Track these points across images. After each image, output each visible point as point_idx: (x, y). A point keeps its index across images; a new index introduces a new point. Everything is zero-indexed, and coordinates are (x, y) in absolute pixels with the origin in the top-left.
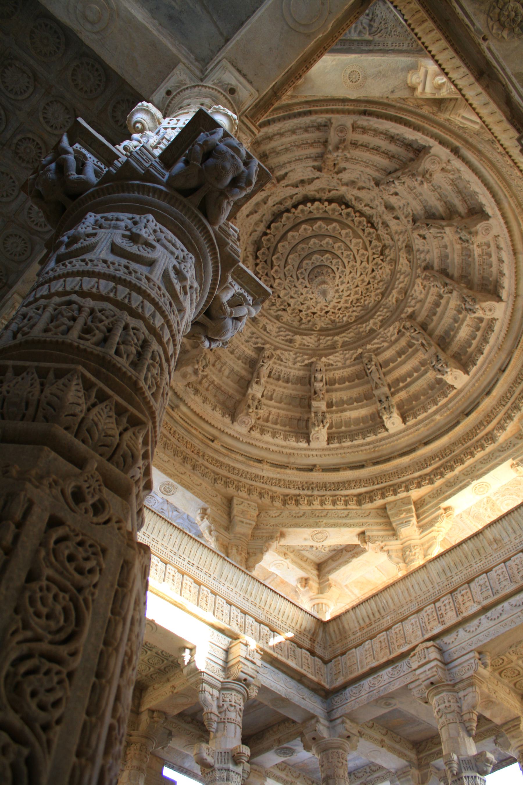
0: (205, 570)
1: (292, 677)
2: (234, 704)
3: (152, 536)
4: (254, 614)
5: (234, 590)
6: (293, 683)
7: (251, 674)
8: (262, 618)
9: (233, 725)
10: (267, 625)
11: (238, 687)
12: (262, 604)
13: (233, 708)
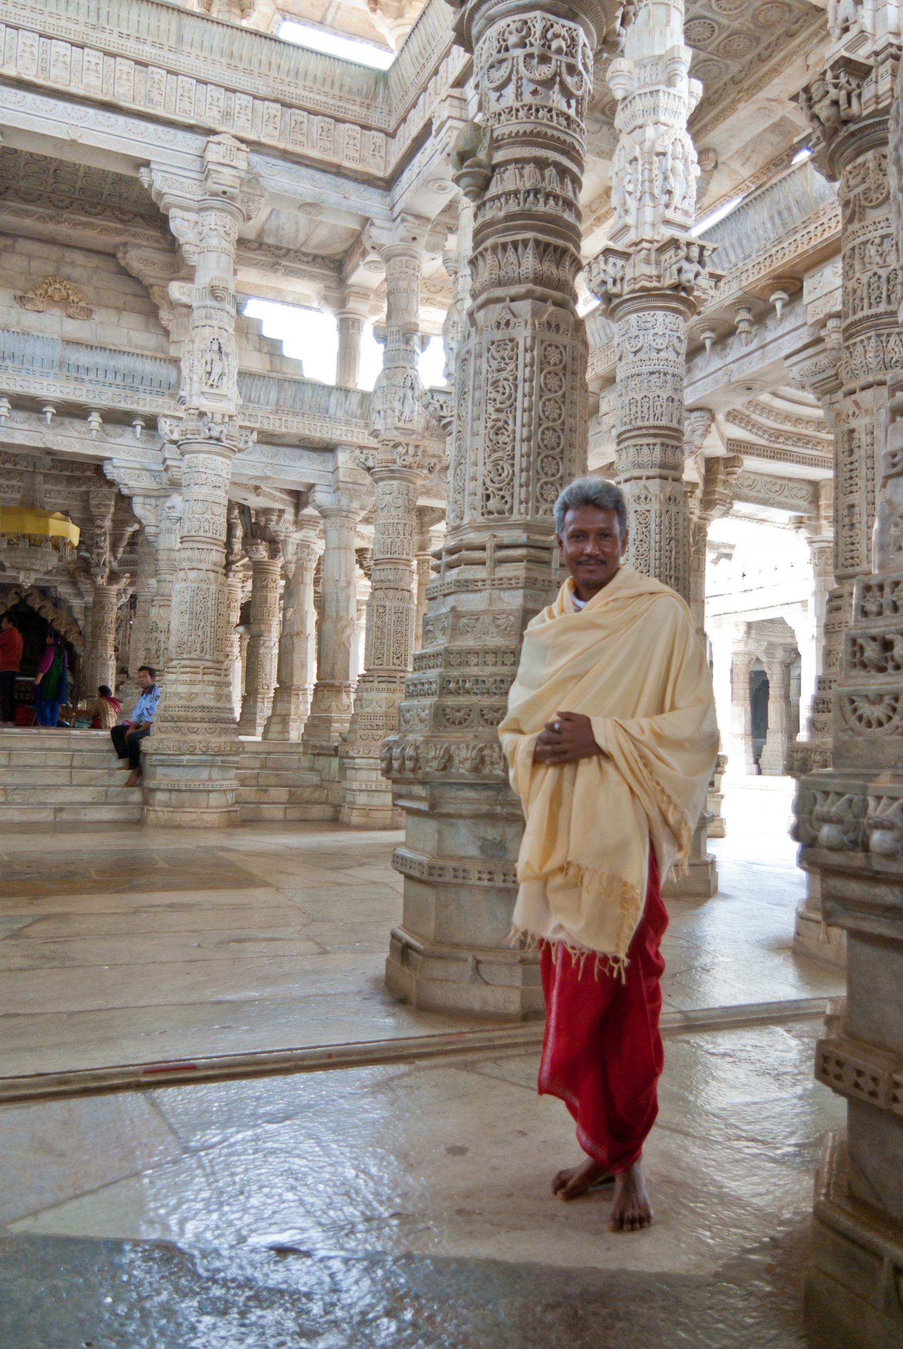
0: (150, 39)
1: (324, 171)
2: (213, 227)
3: (47, 10)
4: (248, 89)
5: (210, 58)
6: (327, 178)
7: (229, 183)
8: (263, 92)
9: (214, 256)
10: (276, 101)
11: (218, 204)
12: (264, 69)
13: (214, 233)
